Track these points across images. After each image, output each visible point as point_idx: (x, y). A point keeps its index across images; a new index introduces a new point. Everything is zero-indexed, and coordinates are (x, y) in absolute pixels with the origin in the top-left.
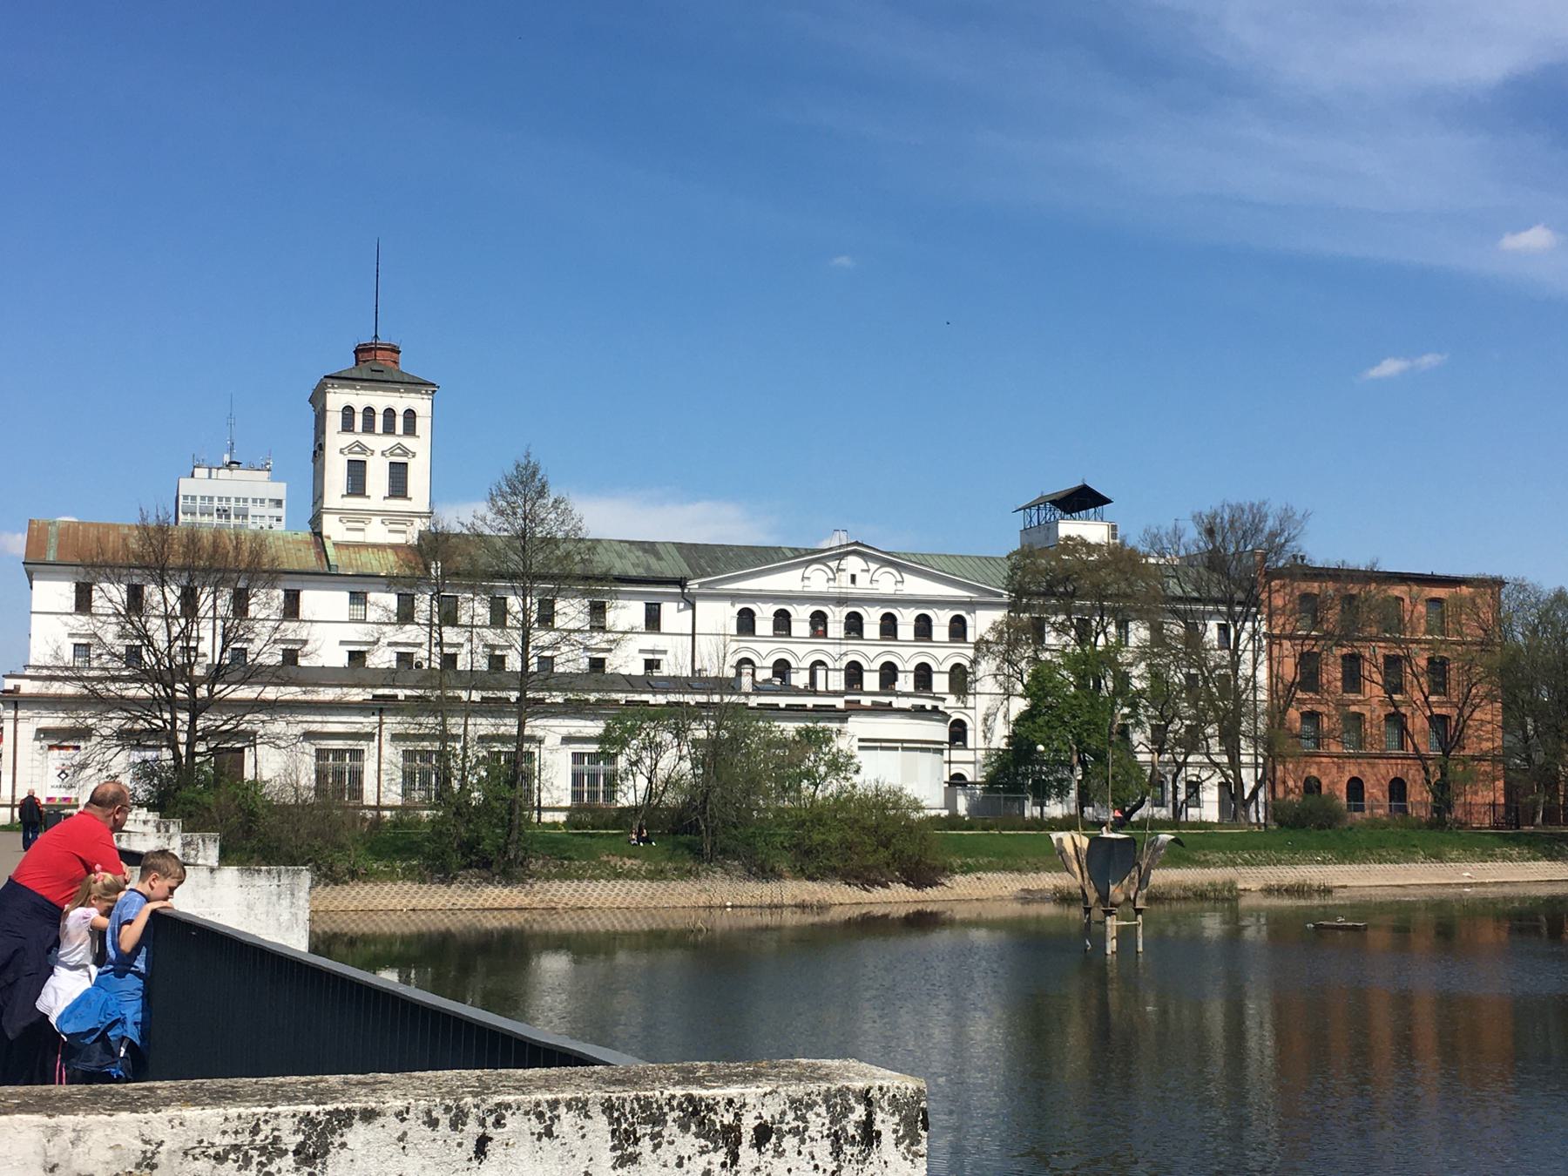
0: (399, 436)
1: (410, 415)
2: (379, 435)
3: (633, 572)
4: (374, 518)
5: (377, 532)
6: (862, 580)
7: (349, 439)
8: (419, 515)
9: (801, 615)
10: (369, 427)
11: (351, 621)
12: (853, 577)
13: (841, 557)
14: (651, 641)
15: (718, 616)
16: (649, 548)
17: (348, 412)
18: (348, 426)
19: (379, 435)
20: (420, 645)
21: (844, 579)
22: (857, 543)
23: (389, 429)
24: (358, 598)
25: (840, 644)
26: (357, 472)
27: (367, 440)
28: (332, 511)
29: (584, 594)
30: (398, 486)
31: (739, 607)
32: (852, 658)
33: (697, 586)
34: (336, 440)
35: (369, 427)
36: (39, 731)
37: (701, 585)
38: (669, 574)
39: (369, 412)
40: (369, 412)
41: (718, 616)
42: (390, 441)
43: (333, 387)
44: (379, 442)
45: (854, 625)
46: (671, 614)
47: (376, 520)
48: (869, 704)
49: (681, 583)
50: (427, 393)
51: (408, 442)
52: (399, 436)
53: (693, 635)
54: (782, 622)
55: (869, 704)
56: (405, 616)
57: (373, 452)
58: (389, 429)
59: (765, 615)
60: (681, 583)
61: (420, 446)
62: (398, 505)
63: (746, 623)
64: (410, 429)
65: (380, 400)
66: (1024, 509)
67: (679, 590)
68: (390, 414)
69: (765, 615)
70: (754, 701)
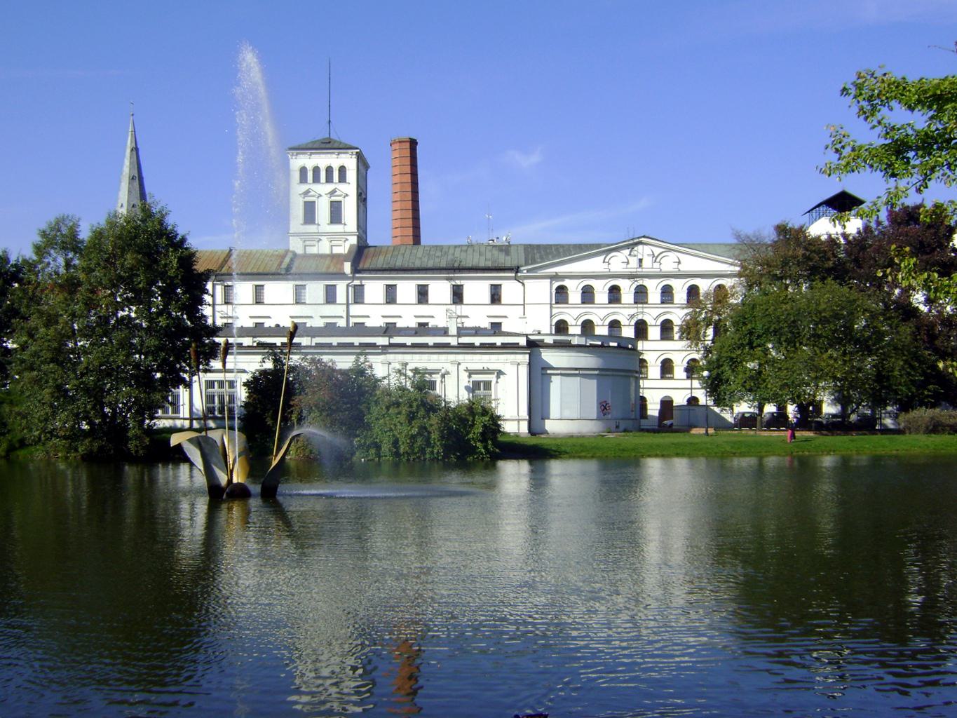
0: (336, 183)
1: (342, 170)
2: (323, 183)
3: (482, 264)
5: (324, 247)
6: (647, 262)
7: (304, 187)
8: (351, 234)
9: (601, 290)
10: (316, 179)
12: (641, 260)
13: (632, 246)
14: (496, 310)
15: (540, 290)
16: (506, 249)
17: (303, 171)
18: (303, 179)
19: (323, 183)
20: (342, 317)
21: (634, 262)
22: (644, 237)
23: (329, 179)
25: (629, 308)
28: (296, 235)
29: (448, 279)
30: (336, 214)
31: (556, 284)
32: (640, 317)
33: (525, 271)
34: (297, 189)
35: (316, 179)
37: (528, 271)
38: (508, 264)
39: (316, 170)
40: (316, 170)
41: (540, 290)
42: (330, 187)
44: (323, 188)
45: (641, 295)
46: (510, 289)
48: (552, 342)
49: (516, 269)
50: (352, 154)
52: (336, 183)
53: (524, 305)
54: (588, 295)
55: (552, 342)
56: (330, 297)
57: (320, 196)
58: (329, 179)
59: (574, 290)
60: (516, 269)
61: (350, 188)
62: (337, 228)
63: (561, 294)
64: (343, 178)
65: (323, 160)
66: (809, 212)
67: (514, 275)
68: (329, 170)
69: (574, 290)
70: (453, 341)
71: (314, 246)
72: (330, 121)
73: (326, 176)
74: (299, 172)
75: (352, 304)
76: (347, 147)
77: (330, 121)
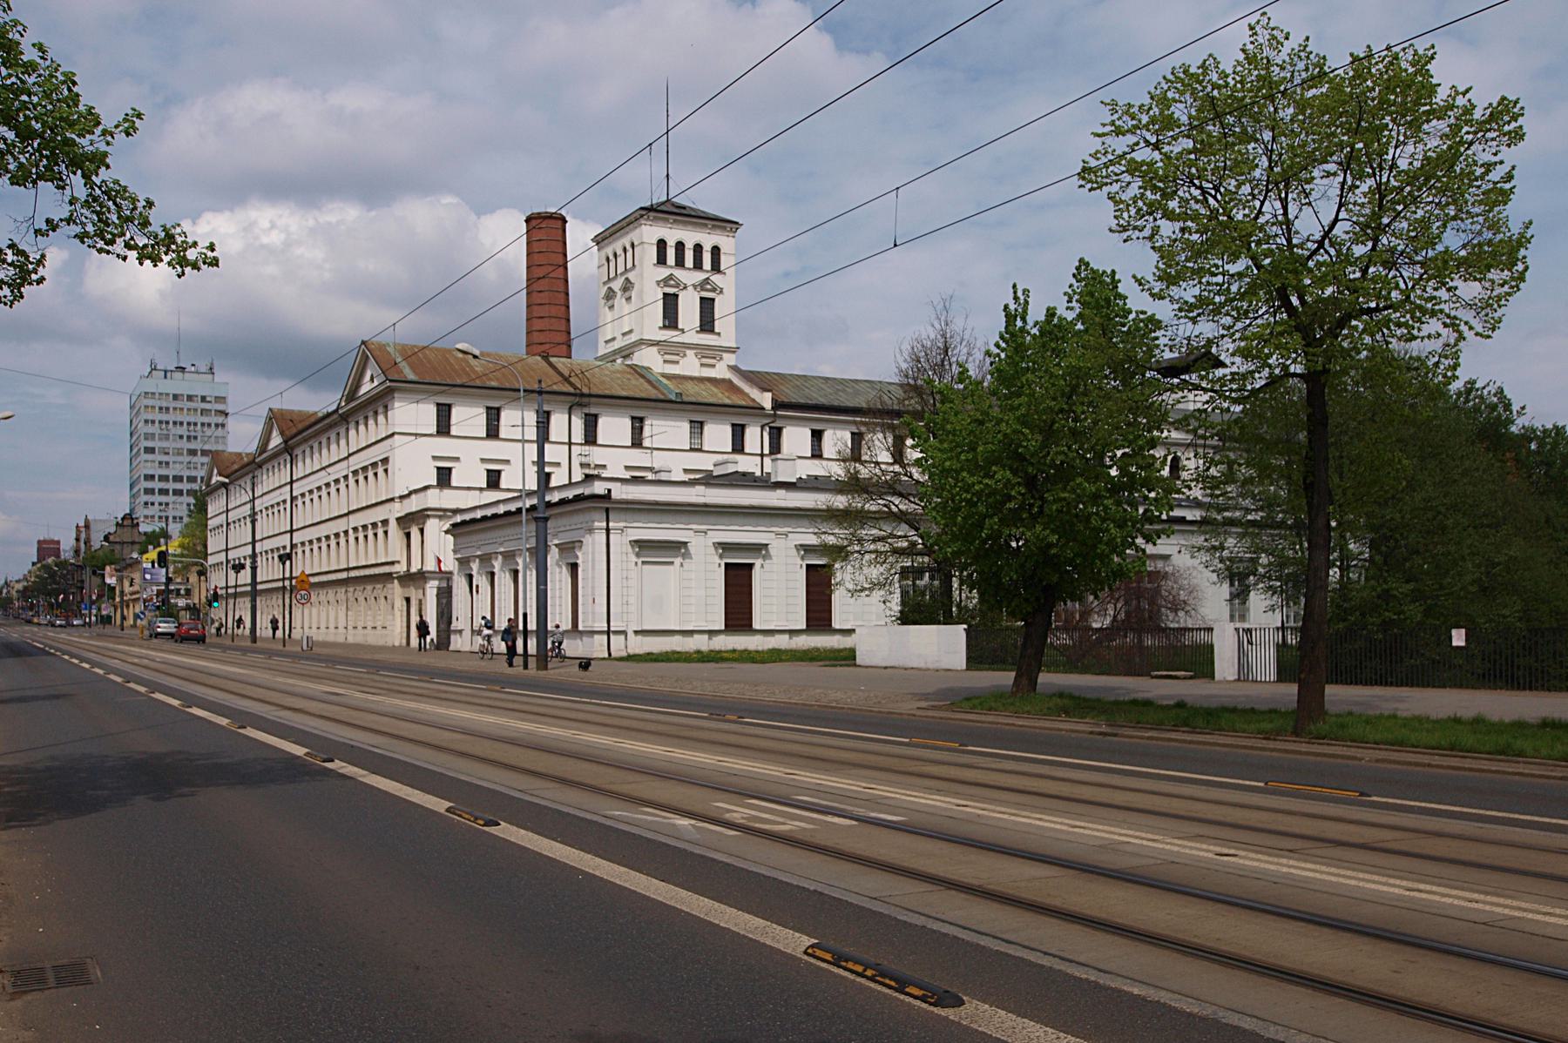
1: (716, 251)
2: (689, 269)
4: (689, 352)
5: (690, 366)
7: (663, 272)
10: (680, 263)
11: (692, 450)
17: (662, 245)
18: (662, 260)
19: (689, 269)
23: (698, 265)
24: (698, 427)
26: (670, 303)
27: (679, 274)
36: (637, 542)
43: (648, 219)
44: (689, 277)
47: (690, 353)
51: (716, 279)
62: (707, 339)
71: (678, 362)
72: (668, 175)
73: (694, 256)
74: (655, 248)
75: (766, 455)
76: (702, 215)
77: (668, 175)
